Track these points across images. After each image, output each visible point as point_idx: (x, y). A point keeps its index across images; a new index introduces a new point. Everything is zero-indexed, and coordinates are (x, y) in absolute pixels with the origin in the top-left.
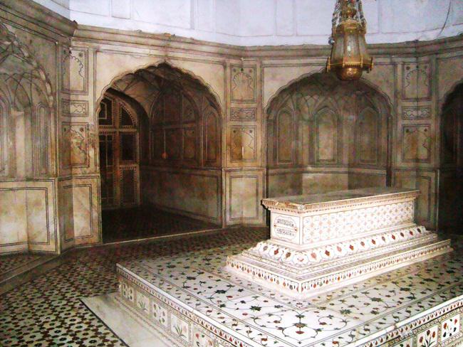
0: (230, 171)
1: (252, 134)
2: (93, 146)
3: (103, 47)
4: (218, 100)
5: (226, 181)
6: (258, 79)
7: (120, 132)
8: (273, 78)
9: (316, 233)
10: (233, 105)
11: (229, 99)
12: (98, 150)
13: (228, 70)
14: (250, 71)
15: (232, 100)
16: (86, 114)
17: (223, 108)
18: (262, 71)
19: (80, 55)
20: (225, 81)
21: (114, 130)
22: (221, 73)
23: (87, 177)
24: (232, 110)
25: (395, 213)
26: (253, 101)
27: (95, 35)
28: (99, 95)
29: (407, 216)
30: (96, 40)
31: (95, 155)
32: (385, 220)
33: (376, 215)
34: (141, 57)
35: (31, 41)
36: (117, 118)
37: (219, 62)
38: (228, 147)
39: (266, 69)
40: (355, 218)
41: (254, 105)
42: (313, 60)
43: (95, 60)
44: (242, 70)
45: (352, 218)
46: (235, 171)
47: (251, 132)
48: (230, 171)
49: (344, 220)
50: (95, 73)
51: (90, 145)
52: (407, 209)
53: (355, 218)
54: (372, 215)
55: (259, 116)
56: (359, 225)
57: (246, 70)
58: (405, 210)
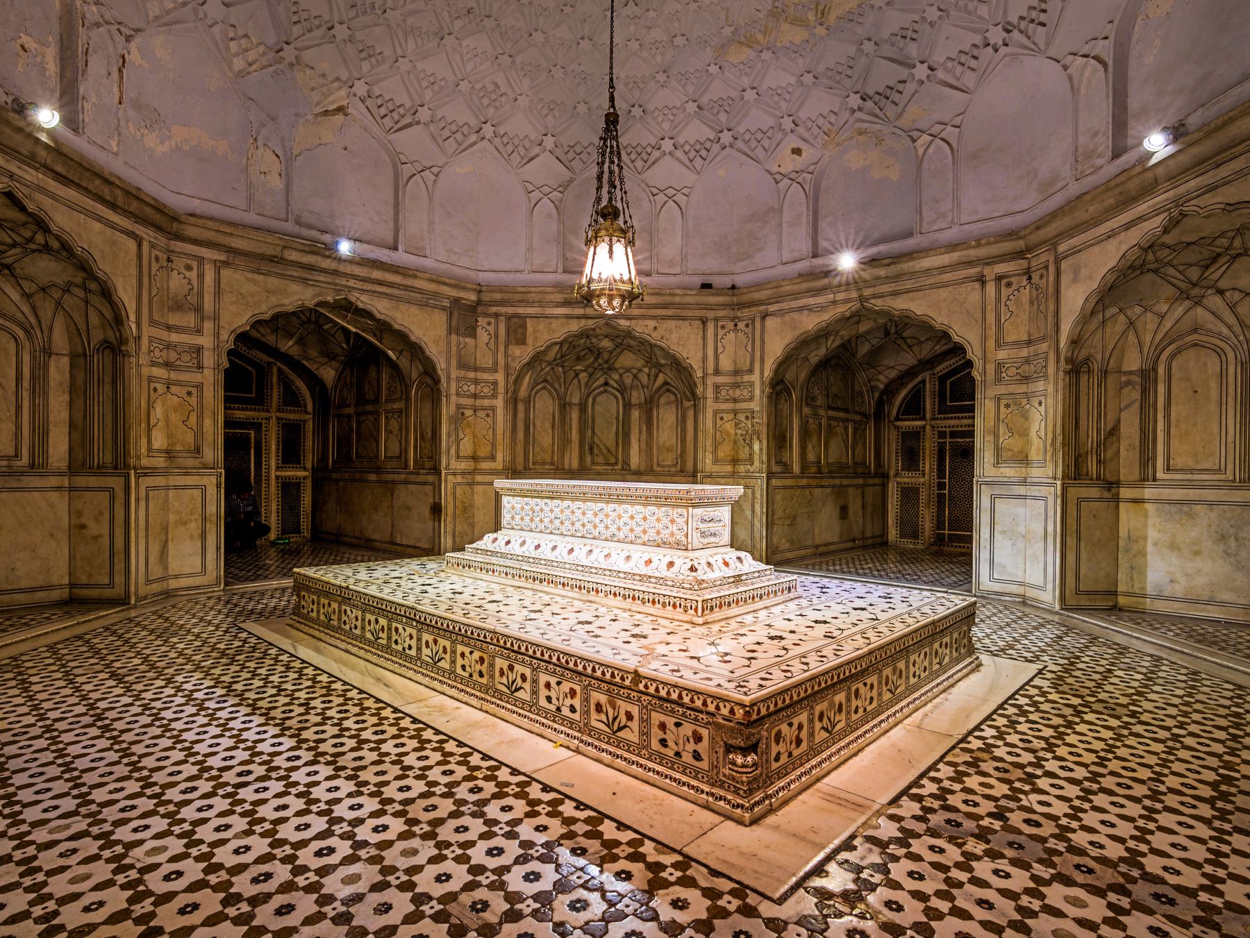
0: (987, 483)
1: (1042, 409)
3: (772, 308)
5: (982, 499)
6: (1051, 289)
8: (1075, 280)
9: (518, 517)
10: (1002, 355)
11: (991, 343)
12: (765, 442)
13: (991, 288)
14: (1042, 276)
15: (999, 344)
16: (751, 399)
17: (978, 363)
18: (1058, 273)
19: (747, 326)
22: (972, 294)
23: (751, 478)
24: (999, 366)
25: (642, 522)
26: (1044, 339)
27: (757, 296)
29: (672, 534)
30: (761, 303)
31: (761, 449)
32: (619, 529)
33: (601, 516)
34: (822, 308)
35: (655, 328)
38: (990, 438)
39: (1064, 265)
40: (567, 512)
41: (1044, 346)
42: (1142, 208)
44: (1030, 278)
45: (562, 511)
47: (1040, 404)
48: (987, 483)
49: (552, 511)
52: (672, 521)
53: (567, 512)
54: (596, 515)
55: (1051, 369)
56: (573, 524)
57: (1035, 277)
58: (666, 521)
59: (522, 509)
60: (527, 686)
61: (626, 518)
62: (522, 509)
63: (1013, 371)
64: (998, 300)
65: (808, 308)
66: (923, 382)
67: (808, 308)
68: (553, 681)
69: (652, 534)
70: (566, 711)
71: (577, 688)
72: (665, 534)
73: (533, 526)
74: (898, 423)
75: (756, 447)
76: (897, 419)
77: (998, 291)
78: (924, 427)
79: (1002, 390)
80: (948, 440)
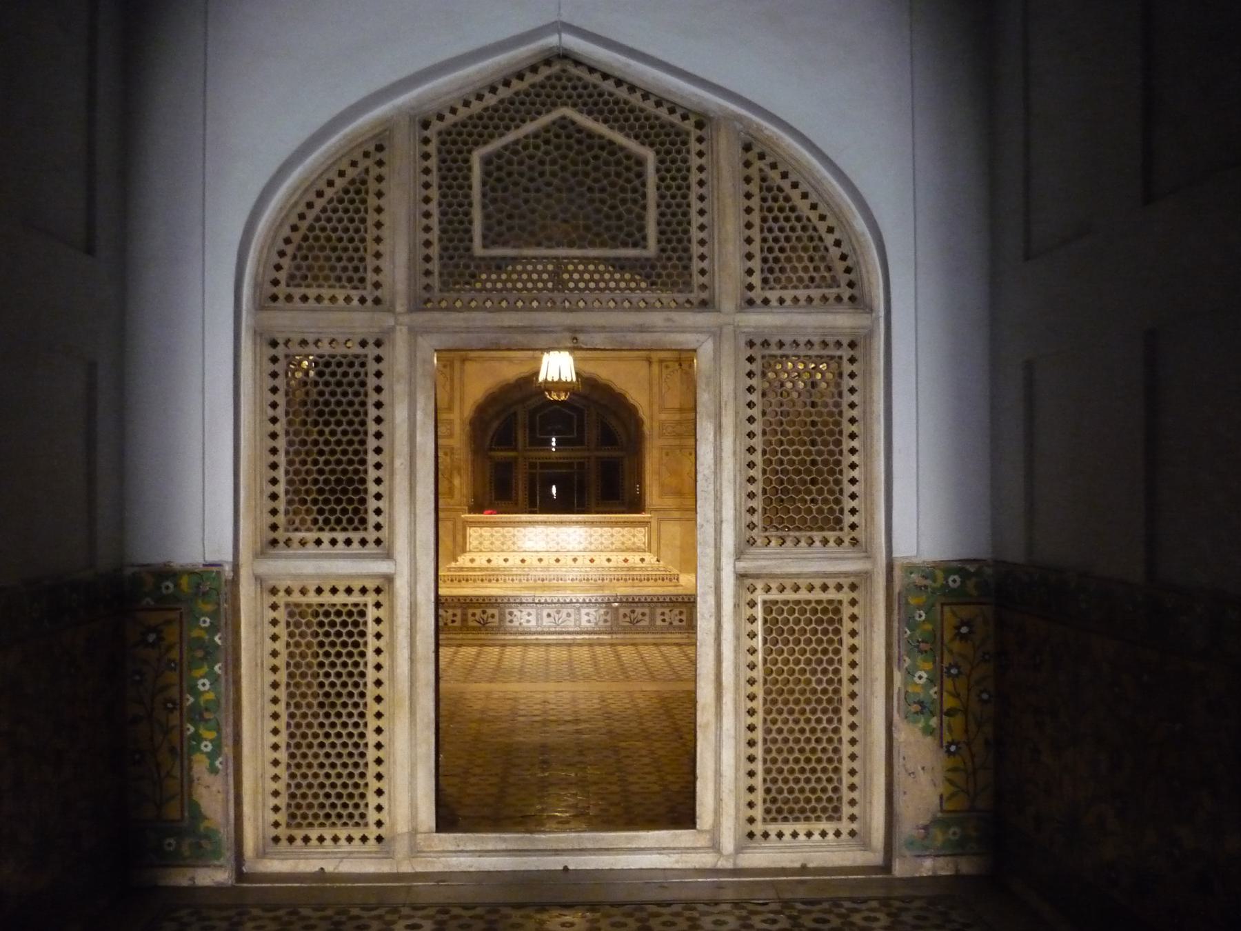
2: (460, 474)
4: (641, 413)
7: (597, 458)
9: (487, 543)
10: (663, 416)
11: (656, 407)
13: (655, 368)
15: (663, 409)
20: (651, 385)
21: (586, 454)
24: (662, 423)
28: (469, 411)
36: (592, 434)
37: (638, 358)
43: (462, 371)
46: (664, 510)
50: (462, 384)
51: (455, 473)
59: (492, 536)
60: (647, 618)
61: (596, 536)
62: (492, 536)
63: (670, 429)
64: (660, 376)
65: (510, 360)
66: (515, 414)
67: (510, 360)
68: (667, 611)
69: (618, 544)
70: (676, 623)
71: (684, 610)
72: (629, 544)
73: (505, 547)
74: (493, 453)
75: (457, 482)
76: (491, 449)
77: (661, 371)
78: (516, 458)
79: (665, 442)
80: (538, 471)
